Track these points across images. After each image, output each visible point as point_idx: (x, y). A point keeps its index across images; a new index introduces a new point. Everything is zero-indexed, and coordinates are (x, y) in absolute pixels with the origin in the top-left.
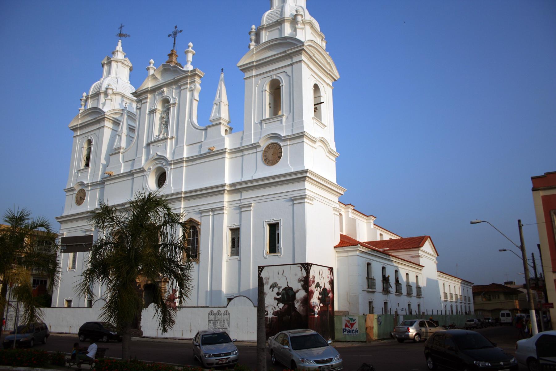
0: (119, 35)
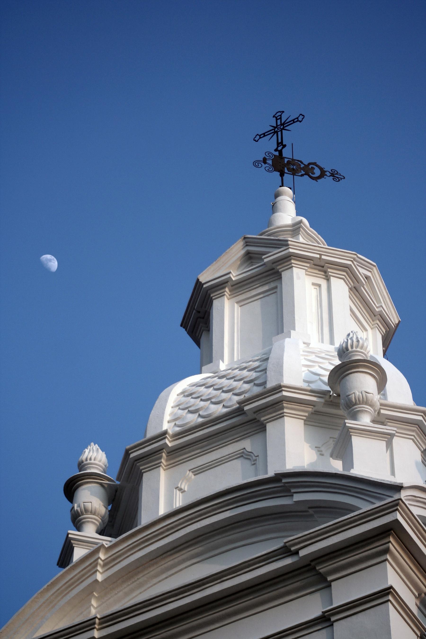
0: (273, 165)
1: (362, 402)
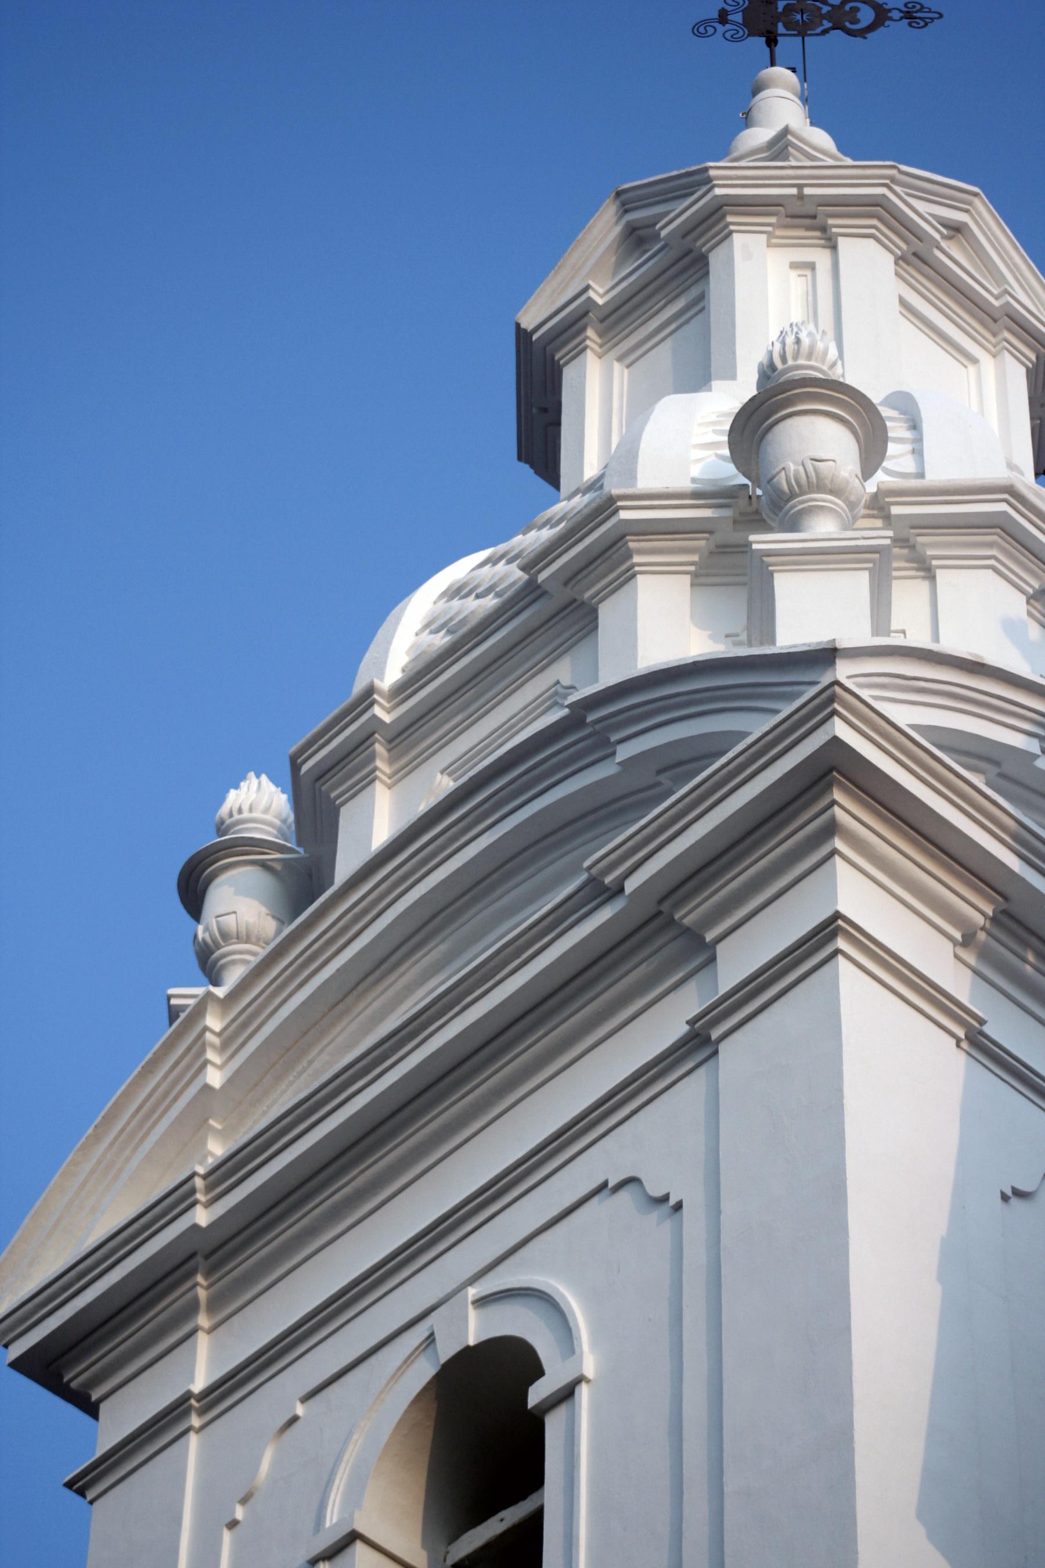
0: (745, 23)
1: (807, 487)
